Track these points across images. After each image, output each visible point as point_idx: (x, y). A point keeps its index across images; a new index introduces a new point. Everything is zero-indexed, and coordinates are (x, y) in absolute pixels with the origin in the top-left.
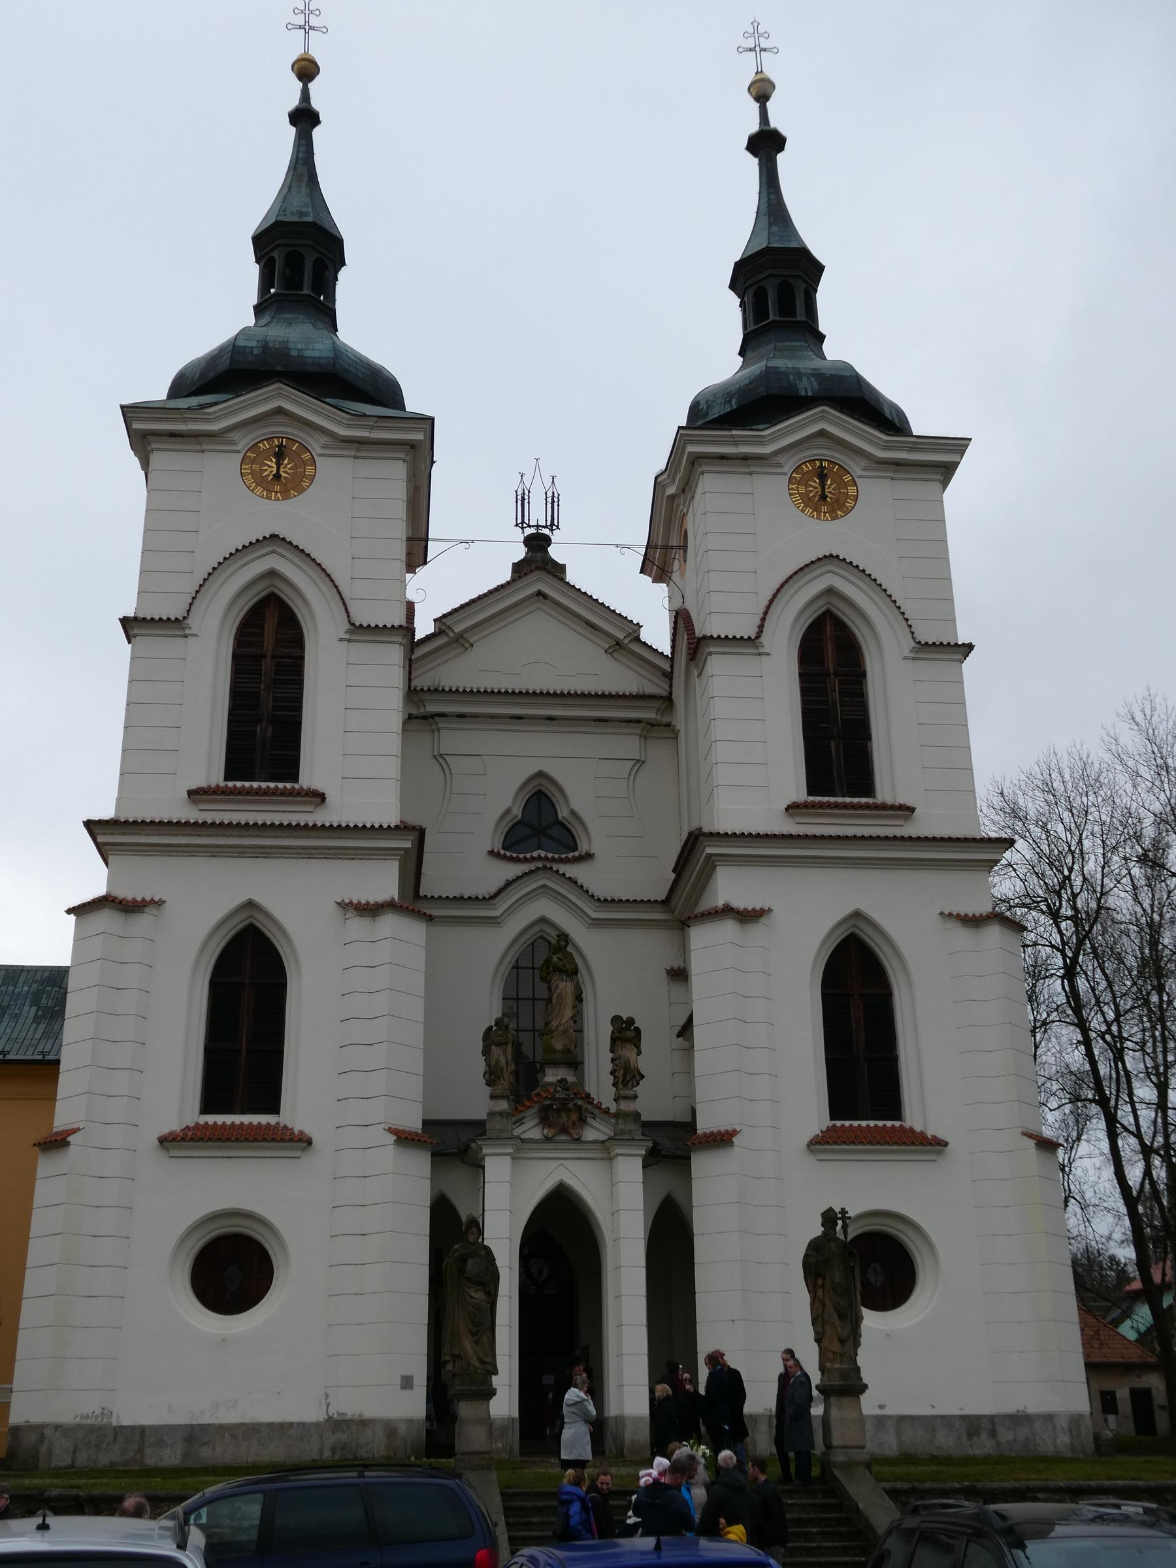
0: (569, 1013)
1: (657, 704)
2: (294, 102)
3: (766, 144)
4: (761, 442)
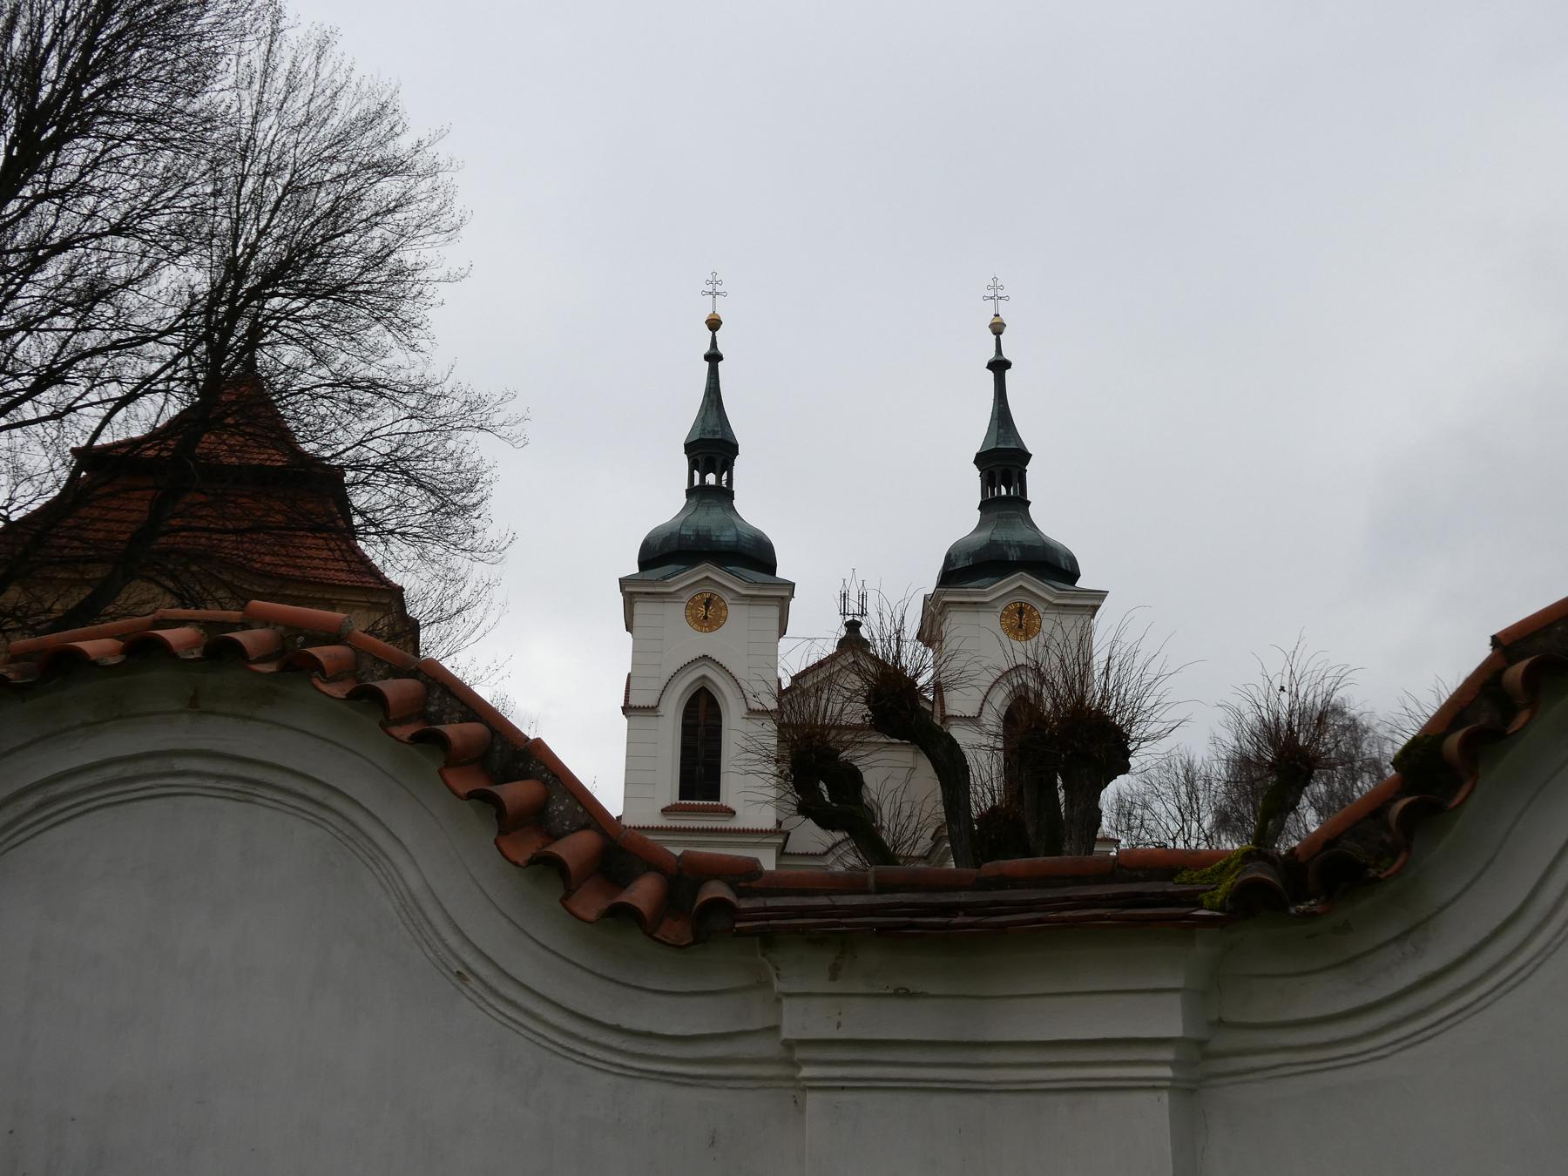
2: (707, 348)
3: (999, 366)
4: (985, 595)
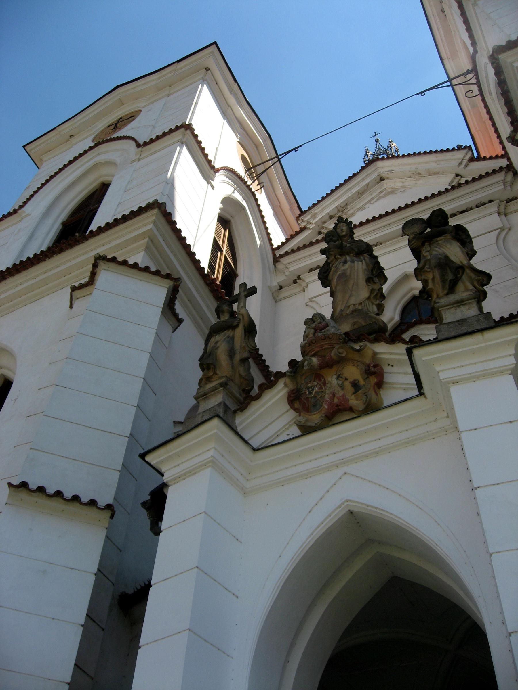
0: (364, 293)
1: (501, 176)
